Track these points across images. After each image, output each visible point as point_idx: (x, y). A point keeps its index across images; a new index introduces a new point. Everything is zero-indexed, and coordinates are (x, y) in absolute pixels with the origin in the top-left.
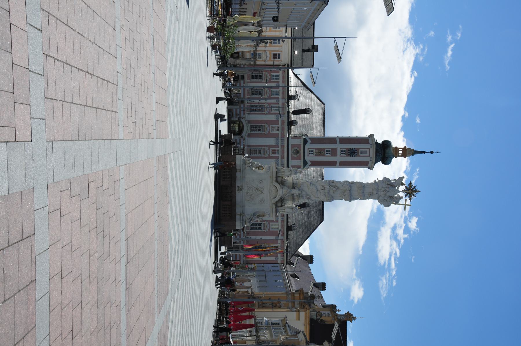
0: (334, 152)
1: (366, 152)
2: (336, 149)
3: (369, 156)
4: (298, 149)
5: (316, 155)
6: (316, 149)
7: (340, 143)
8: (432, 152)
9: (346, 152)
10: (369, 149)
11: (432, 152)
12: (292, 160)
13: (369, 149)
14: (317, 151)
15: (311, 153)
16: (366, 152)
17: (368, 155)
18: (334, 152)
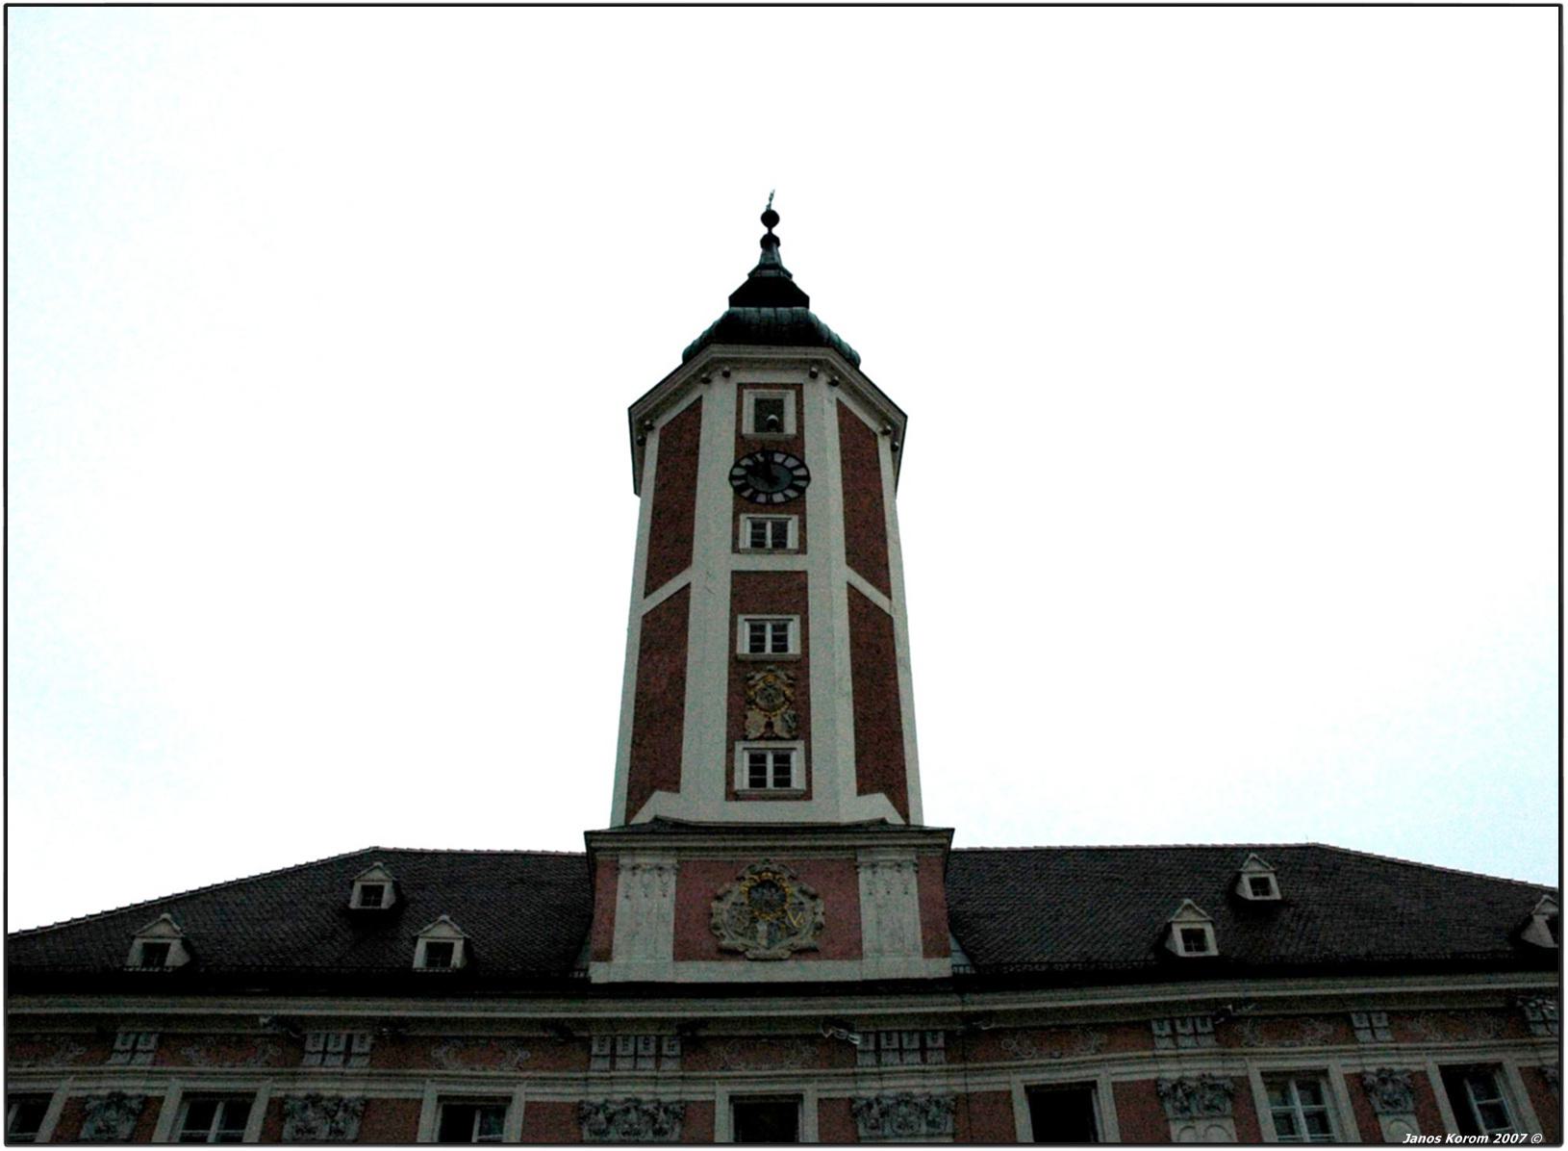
0: (770, 597)
1: (768, 412)
2: (738, 577)
3: (799, 389)
4: (738, 892)
5: (801, 728)
6: (737, 731)
7: (685, 562)
8: (770, 218)
9: (769, 520)
10: (741, 387)
11: (770, 218)
12: (853, 950)
13: (741, 387)
14: (756, 719)
15: (771, 775)
16: (768, 412)
17: (790, 398)
18: (770, 597)
